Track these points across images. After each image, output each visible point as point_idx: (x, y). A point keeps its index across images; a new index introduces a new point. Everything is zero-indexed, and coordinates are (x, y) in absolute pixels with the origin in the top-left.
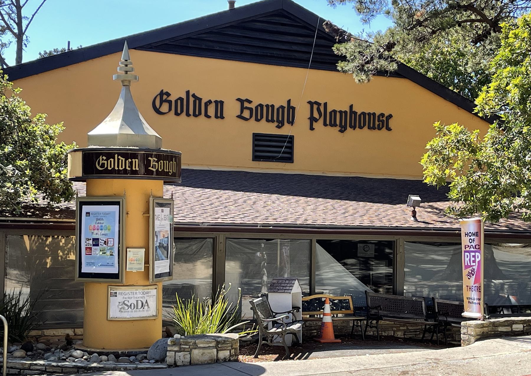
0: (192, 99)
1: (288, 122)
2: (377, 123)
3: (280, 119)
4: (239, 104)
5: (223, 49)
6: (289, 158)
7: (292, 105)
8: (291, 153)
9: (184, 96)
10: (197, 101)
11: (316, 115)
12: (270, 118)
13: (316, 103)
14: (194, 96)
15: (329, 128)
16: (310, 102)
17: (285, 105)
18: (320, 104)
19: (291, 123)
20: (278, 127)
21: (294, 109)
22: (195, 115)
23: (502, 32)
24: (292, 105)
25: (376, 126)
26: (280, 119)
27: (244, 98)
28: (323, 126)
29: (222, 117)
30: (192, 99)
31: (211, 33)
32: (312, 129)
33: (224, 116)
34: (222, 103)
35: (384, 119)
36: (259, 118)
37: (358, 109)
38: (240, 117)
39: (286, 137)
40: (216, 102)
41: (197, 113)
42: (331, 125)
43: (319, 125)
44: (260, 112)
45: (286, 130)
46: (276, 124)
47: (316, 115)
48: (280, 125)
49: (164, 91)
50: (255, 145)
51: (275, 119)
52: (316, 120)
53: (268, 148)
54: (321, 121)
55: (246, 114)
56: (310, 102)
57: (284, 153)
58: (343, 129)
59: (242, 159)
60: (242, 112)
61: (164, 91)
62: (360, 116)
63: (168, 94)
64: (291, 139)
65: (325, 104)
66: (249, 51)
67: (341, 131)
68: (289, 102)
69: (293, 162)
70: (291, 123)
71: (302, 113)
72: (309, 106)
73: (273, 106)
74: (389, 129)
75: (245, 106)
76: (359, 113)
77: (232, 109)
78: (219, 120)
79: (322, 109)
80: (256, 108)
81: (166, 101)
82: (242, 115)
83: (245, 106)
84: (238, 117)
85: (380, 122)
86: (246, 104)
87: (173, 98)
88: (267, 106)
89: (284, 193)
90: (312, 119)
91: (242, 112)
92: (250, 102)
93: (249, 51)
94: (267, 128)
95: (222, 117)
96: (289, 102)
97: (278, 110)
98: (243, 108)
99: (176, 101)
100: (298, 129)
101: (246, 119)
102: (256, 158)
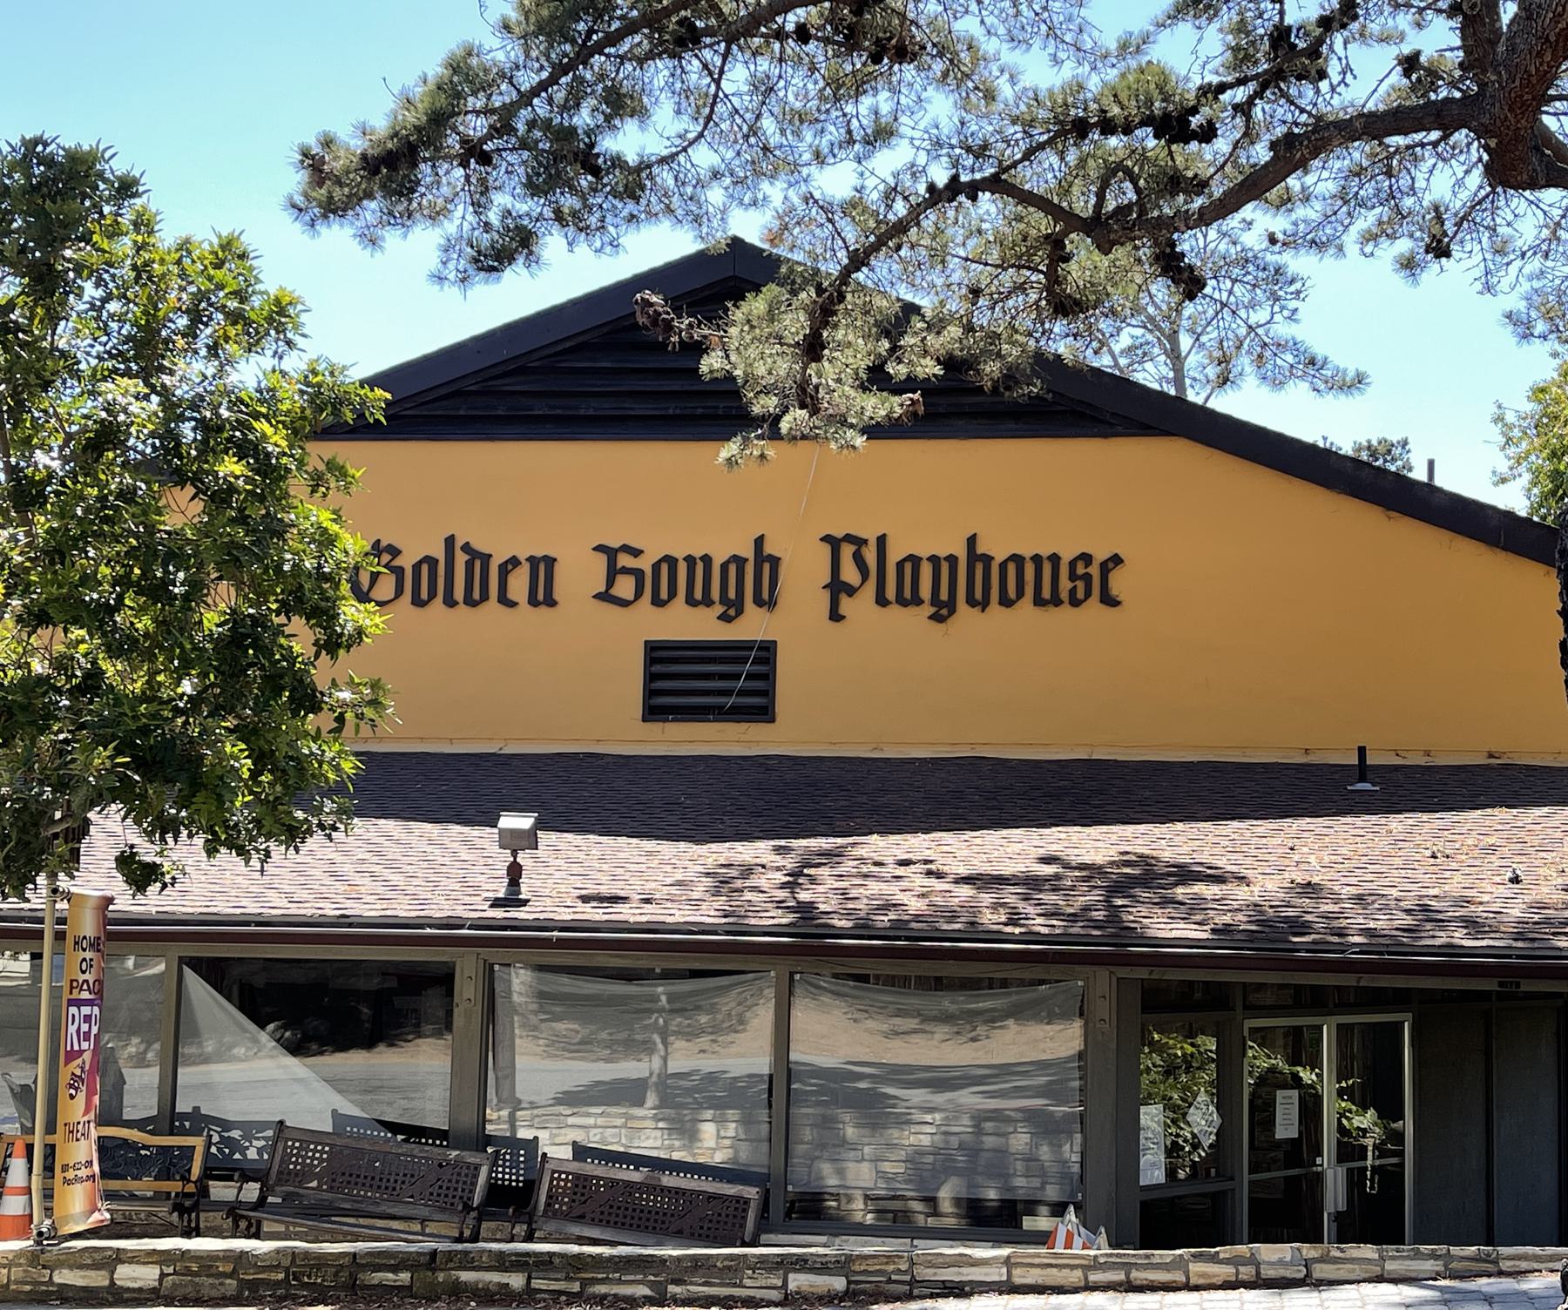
0: (461, 558)
1: (759, 602)
2: (1065, 584)
3: (732, 594)
4: (601, 561)
5: (559, 412)
6: (764, 712)
7: (769, 549)
8: (769, 693)
9: (439, 553)
10: (478, 564)
11: (850, 574)
12: (698, 595)
13: (849, 538)
14: (466, 548)
15: (895, 610)
16: (827, 539)
17: (748, 552)
18: (865, 542)
19: (767, 602)
20: (725, 618)
21: (775, 562)
22: (470, 602)
23: (1427, 252)
24: (981, 549)
25: (1064, 595)
26: (732, 594)
27: (615, 544)
28: (654, 608)
29: (551, 602)
30: (461, 558)
31: (522, 370)
32: (835, 616)
33: (556, 597)
34: (550, 562)
35: (1094, 570)
36: (424, 595)
37: (997, 548)
38: (605, 597)
39: (746, 646)
40: (532, 560)
41: (476, 595)
42: (902, 601)
43: (860, 607)
44: (665, 580)
45: (752, 626)
46: (719, 609)
47: (850, 574)
48: (732, 612)
49: (384, 544)
50: (650, 677)
51: (715, 594)
52: (851, 591)
53: (681, 681)
54: (870, 588)
55: (625, 587)
56: (827, 539)
57: (743, 693)
58: (944, 612)
59: (615, 723)
60: (610, 582)
61: (384, 544)
62: (1003, 566)
63: (394, 552)
64: (766, 652)
65: (882, 540)
66: (640, 409)
67: (937, 618)
68: (759, 542)
69: (773, 720)
70: (767, 602)
71: (805, 572)
72: (826, 549)
73: (707, 560)
74: (1109, 601)
75: (619, 566)
76: (1000, 555)
77: (580, 575)
78: (543, 610)
79: (870, 556)
80: (656, 567)
81: (626, 571)
82: (613, 592)
83: (619, 566)
84: (598, 596)
85: (1084, 581)
86: (624, 560)
87: (406, 561)
88: (690, 560)
89: (519, 806)
90: (837, 588)
91: (610, 582)
92: (636, 553)
93: (640, 409)
94: (688, 624)
95: (551, 602)
96: (759, 542)
97: (724, 567)
98: (613, 573)
99: (417, 567)
100: (792, 625)
101: (624, 603)
102: (654, 711)
